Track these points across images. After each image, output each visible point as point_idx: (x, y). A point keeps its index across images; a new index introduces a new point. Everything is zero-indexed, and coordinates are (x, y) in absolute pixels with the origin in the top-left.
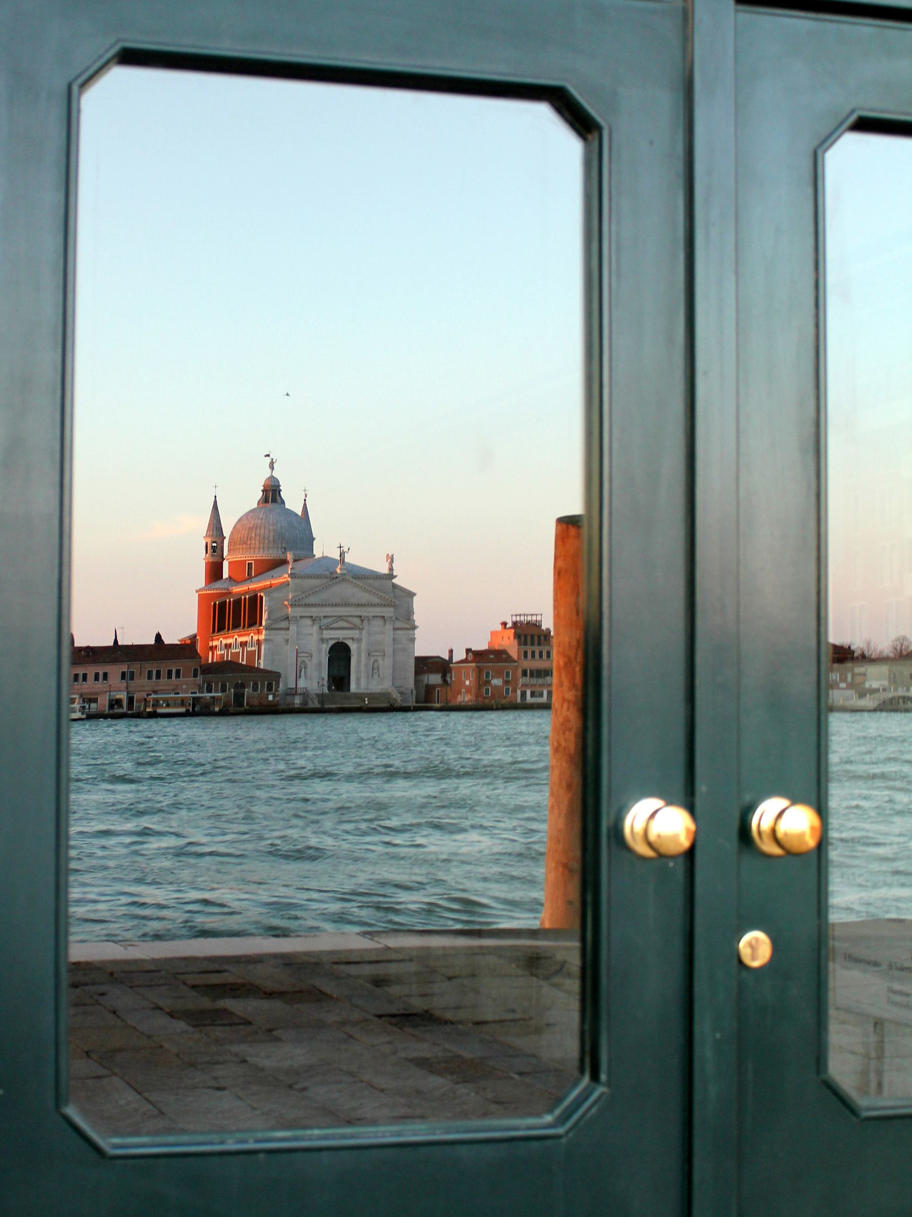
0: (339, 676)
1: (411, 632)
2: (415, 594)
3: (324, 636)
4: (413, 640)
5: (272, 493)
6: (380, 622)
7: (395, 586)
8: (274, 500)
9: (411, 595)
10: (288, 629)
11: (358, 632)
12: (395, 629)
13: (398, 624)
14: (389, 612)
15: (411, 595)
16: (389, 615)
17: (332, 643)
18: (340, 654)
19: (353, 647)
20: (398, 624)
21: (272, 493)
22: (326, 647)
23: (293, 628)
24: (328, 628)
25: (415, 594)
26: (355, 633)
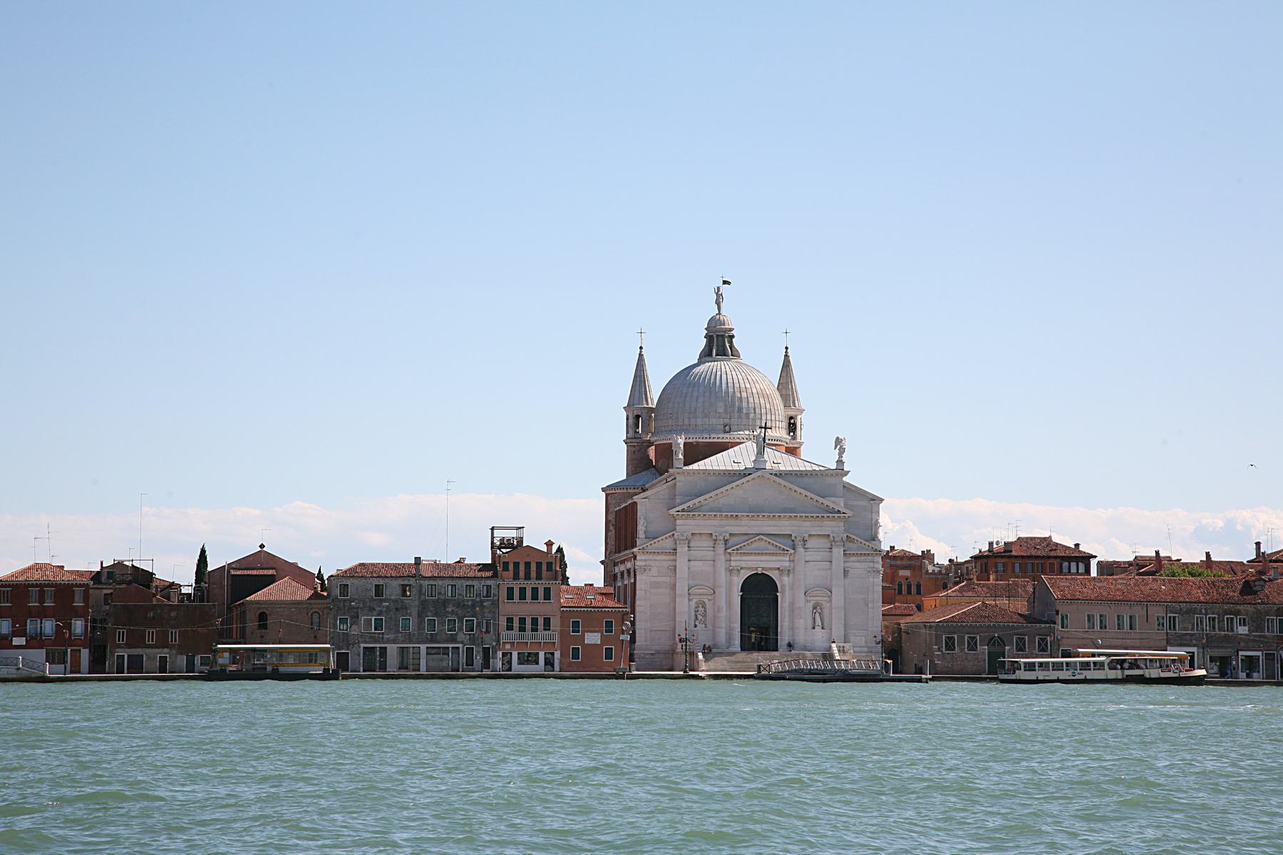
5: (719, 342)
6: (824, 543)
7: (849, 488)
8: (722, 353)
12: (845, 554)
14: (833, 527)
17: (745, 575)
21: (719, 342)
22: (738, 581)
23: (682, 549)
26: (784, 562)
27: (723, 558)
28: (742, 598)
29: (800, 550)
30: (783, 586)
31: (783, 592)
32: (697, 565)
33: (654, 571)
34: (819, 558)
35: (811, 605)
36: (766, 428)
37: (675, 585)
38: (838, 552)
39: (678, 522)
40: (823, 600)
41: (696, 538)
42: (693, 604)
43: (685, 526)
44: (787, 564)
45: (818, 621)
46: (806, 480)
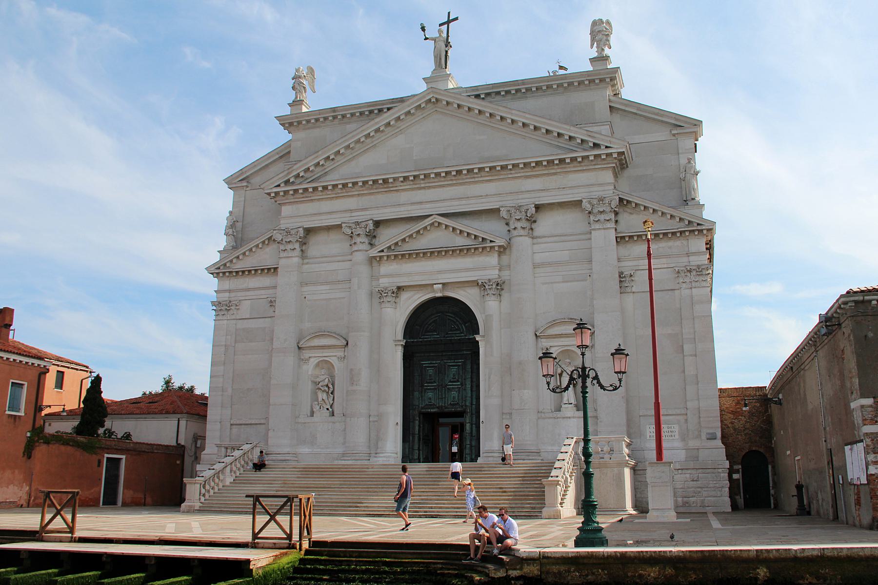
3: (384, 282)
7: (624, 110)
9: (686, 129)
11: (492, 259)
12: (620, 240)
15: (686, 129)
16: (597, 192)
17: (411, 301)
19: (487, 310)
22: (398, 315)
25: (697, 124)
26: (486, 266)
27: (364, 270)
29: (522, 242)
30: (488, 318)
33: (245, 309)
36: (448, 22)
37: (273, 331)
38: (604, 236)
41: (321, 237)
42: (309, 368)
44: (493, 274)
46: (532, 103)
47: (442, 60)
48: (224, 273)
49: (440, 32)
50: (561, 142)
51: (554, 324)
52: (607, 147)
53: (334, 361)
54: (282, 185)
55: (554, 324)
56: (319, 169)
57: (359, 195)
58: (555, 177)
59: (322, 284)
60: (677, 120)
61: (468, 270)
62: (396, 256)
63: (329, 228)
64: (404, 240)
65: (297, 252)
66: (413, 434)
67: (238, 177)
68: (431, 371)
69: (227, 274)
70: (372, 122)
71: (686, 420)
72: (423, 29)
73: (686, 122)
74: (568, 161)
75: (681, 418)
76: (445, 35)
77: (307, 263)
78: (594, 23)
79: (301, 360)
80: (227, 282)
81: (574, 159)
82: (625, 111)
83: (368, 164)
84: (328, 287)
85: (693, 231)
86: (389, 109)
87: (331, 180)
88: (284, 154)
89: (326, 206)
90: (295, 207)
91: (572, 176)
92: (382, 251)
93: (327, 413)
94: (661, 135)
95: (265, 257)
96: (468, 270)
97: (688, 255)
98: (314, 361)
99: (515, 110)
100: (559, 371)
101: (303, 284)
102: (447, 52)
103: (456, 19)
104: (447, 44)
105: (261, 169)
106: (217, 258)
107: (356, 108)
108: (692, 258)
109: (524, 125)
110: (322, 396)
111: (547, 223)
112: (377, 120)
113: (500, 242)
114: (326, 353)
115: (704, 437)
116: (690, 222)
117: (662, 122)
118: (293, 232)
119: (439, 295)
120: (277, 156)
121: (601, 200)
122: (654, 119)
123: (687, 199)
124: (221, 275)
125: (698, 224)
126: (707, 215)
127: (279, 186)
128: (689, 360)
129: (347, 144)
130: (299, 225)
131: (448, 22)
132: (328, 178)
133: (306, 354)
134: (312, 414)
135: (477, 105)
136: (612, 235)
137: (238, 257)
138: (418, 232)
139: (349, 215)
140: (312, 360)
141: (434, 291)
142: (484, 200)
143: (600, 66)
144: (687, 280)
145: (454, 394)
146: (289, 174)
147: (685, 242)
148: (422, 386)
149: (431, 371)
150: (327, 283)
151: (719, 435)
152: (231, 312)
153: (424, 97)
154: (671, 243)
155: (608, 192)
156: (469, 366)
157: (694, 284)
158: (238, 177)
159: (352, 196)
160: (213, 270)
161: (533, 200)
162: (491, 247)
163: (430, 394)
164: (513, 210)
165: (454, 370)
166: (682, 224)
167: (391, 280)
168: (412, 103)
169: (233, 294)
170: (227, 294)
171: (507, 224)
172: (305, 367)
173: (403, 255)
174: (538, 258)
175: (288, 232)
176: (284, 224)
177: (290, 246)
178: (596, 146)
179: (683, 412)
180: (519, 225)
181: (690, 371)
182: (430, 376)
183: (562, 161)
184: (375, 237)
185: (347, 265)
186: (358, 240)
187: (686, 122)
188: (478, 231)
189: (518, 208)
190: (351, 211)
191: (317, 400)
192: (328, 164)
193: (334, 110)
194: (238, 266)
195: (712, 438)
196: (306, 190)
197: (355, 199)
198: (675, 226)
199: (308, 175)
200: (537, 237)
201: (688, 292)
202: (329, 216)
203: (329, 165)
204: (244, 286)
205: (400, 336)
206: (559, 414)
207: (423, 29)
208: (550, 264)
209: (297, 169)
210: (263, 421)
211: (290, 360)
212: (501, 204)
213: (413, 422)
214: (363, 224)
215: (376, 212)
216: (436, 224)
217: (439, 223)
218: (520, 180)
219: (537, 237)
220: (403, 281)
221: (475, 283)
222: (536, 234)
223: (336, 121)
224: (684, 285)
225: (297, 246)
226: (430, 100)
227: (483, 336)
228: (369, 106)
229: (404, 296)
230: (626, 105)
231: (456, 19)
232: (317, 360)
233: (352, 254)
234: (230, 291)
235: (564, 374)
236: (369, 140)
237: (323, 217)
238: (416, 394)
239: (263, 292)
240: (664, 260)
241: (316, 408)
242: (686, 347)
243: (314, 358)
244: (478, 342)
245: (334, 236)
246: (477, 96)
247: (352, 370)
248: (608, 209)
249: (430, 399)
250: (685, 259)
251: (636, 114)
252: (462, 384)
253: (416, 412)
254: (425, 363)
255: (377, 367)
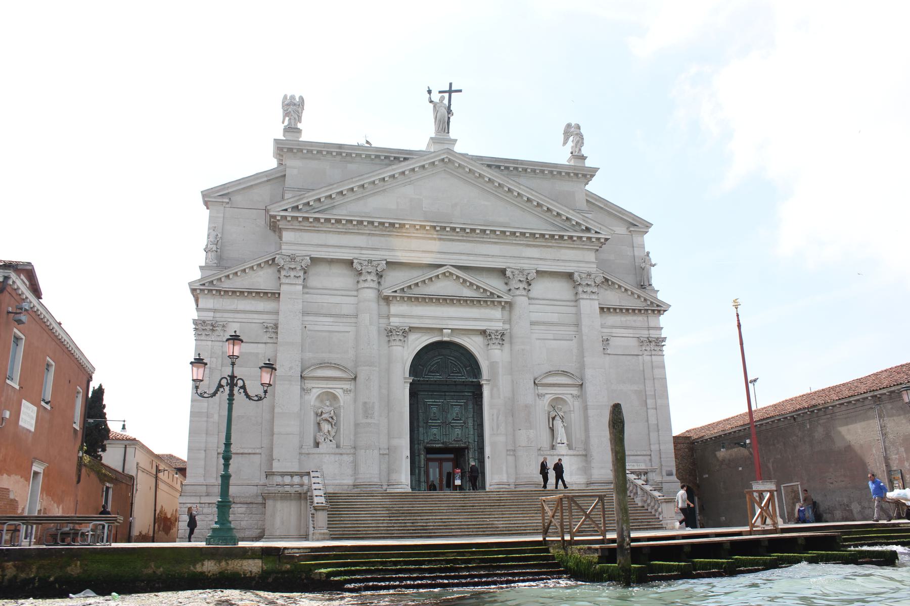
0: (447, 452)
1: (652, 321)
2: (648, 225)
3: (395, 321)
4: (659, 342)
6: (560, 289)
10: (275, 296)
11: (497, 313)
12: (602, 309)
13: (612, 298)
16: (585, 268)
17: (418, 342)
18: (445, 380)
20: (612, 298)
23: (291, 289)
24: (408, 296)
25: (648, 225)
26: (492, 319)
28: (413, 394)
29: (521, 301)
30: (493, 366)
31: (492, 380)
32: (324, 324)
34: (554, 318)
35: (544, 404)
36: (450, 92)
38: (589, 306)
39: (287, 236)
40: (568, 393)
41: (323, 269)
42: (312, 398)
43: (297, 242)
44: (499, 326)
45: (561, 435)
47: (444, 123)
48: (210, 291)
49: (442, 98)
50: (557, 221)
51: (549, 374)
52: (596, 232)
53: (339, 393)
54: (290, 210)
55: (549, 374)
56: (329, 201)
57: (369, 234)
58: (550, 249)
59: (325, 315)
60: (634, 219)
61: (475, 319)
62: (410, 298)
63: (331, 262)
64: (417, 284)
65: (300, 281)
66: (419, 467)
67: (218, 191)
68: (434, 409)
69: (214, 292)
70: (390, 168)
71: (651, 460)
72: (429, 92)
73: (640, 223)
74: (566, 238)
75: (648, 458)
76: (446, 102)
77: (307, 293)
78: (569, 126)
79: (303, 389)
80: (212, 301)
81: (571, 237)
82: (594, 204)
83: (378, 205)
84: (331, 319)
85: (653, 311)
86: (405, 159)
87: (341, 213)
88: (276, 178)
89: (333, 239)
90: (298, 234)
91: (563, 251)
92: (396, 292)
93: (333, 445)
94: (621, 230)
95: (263, 279)
96: (475, 319)
97: (649, 328)
98: (316, 392)
99: (524, 186)
100: (553, 414)
101: (305, 313)
102: (449, 118)
103: (460, 91)
104: (449, 111)
105: (244, 189)
106: (197, 275)
107: (363, 150)
108: (651, 332)
109: (529, 200)
110: (326, 427)
111: (541, 288)
112: (394, 167)
113: (506, 298)
114: (331, 385)
115: (664, 473)
116: (652, 303)
117: (622, 219)
118: (298, 259)
119: (445, 339)
120: (266, 179)
121: (589, 275)
122: (616, 215)
123: (644, 284)
124: (206, 292)
125: (658, 306)
126: (661, 296)
127: (286, 210)
128: (651, 412)
129: (362, 183)
130: (304, 253)
131: (450, 92)
132: (335, 211)
133: (309, 384)
134: (317, 445)
135: (488, 173)
136: (596, 306)
137: (228, 276)
138: (431, 279)
139: (358, 251)
140: (314, 390)
141: (442, 335)
142: (490, 259)
143: (579, 164)
144: (648, 348)
145: (458, 431)
146: (298, 200)
147: (646, 319)
148: (427, 422)
149: (434, 409)
150: (331, 315)
151: (674, 472)
152: (216, 333)
153: (439, 155)
154: (635, 318)
155: (592, 268)
156: (471, 406)
157: (653, 353)
158: (218, 191)
159: (363, 234)
160: (197, 286)
161: (536, 266)
162: (500, 302)
163: (435, 431)
164: (517, 272)
165: (457, 409)
166: (645, 304)
167: (402, 320)
168: (428, 159)
169: (218, 315)
170: (211, 314)
171: (506, 284)
172: (307, 397)
173: (417, 299)
174: (535, 317)
175: (293, 258)
176: (286, 250)
177: (292, 274)
178: (588, 230)
179: (648, 453)
180: (521, 286)
181: (652, 421)
182: (434, 413)
183: (561, 237)
184: (381, 276)
185: (353, 300)
186: (369, 278)
187: (640, 223)
188: (493, 287)
189: (521, 271)
190: (361, 248)
191: (320, 429)
192: (339, 198)
193: (340, 146)
194: (226, 285)
195: (670, 474)
196: (317, 220)
197: (364, 237)
198: (639, 304)
199: (317, 205)
200: (534, 299)
201: (649, 357)
202: (338, 250)
203: (339, 200)
204: (233, 307)
205: (407, 375)
206: (555, 452)
207: (429, 92)
208: (544, 323)
209: (307, 197)
210: (258, 451)
211: (296, 388)
212: (508, 265)
213: (419, 456)
214: (374, 263)
215: (387, 253)
216: (447, 274)
217: (451, 274)
218: (521, 248)
219: (534, 299)
220: (416, 323)
221: (483, 333)
222: (533, 294)
223: (339, 158)
224: (646, 353)
225: (301, 274)
226: (443, 160)
227: (488, 380)
228: (377, 151)
229: (412, 337)
230: (596, 200)
231: (460, 91)
232: (320, 391)
233: (357, 290)
234: (215, 311)
235: (558, 418)
236: (382, 183)
237: (330, 250)
238: (421, 429)
239: (256, 316)
240: (631, 331)
241: (321, 440)
242: (649, 401)
243: (317, 389)
244: (479, 387)
245: (336, 270)
246: (489, 166)
247: (365, 403)
248: (593, 284)
249: (435, 435)
250: (646, 332)
251: (602, 208)
252: (464, 423)
253: (421, 447)
254: (429, 401)
255: (388, 404)
